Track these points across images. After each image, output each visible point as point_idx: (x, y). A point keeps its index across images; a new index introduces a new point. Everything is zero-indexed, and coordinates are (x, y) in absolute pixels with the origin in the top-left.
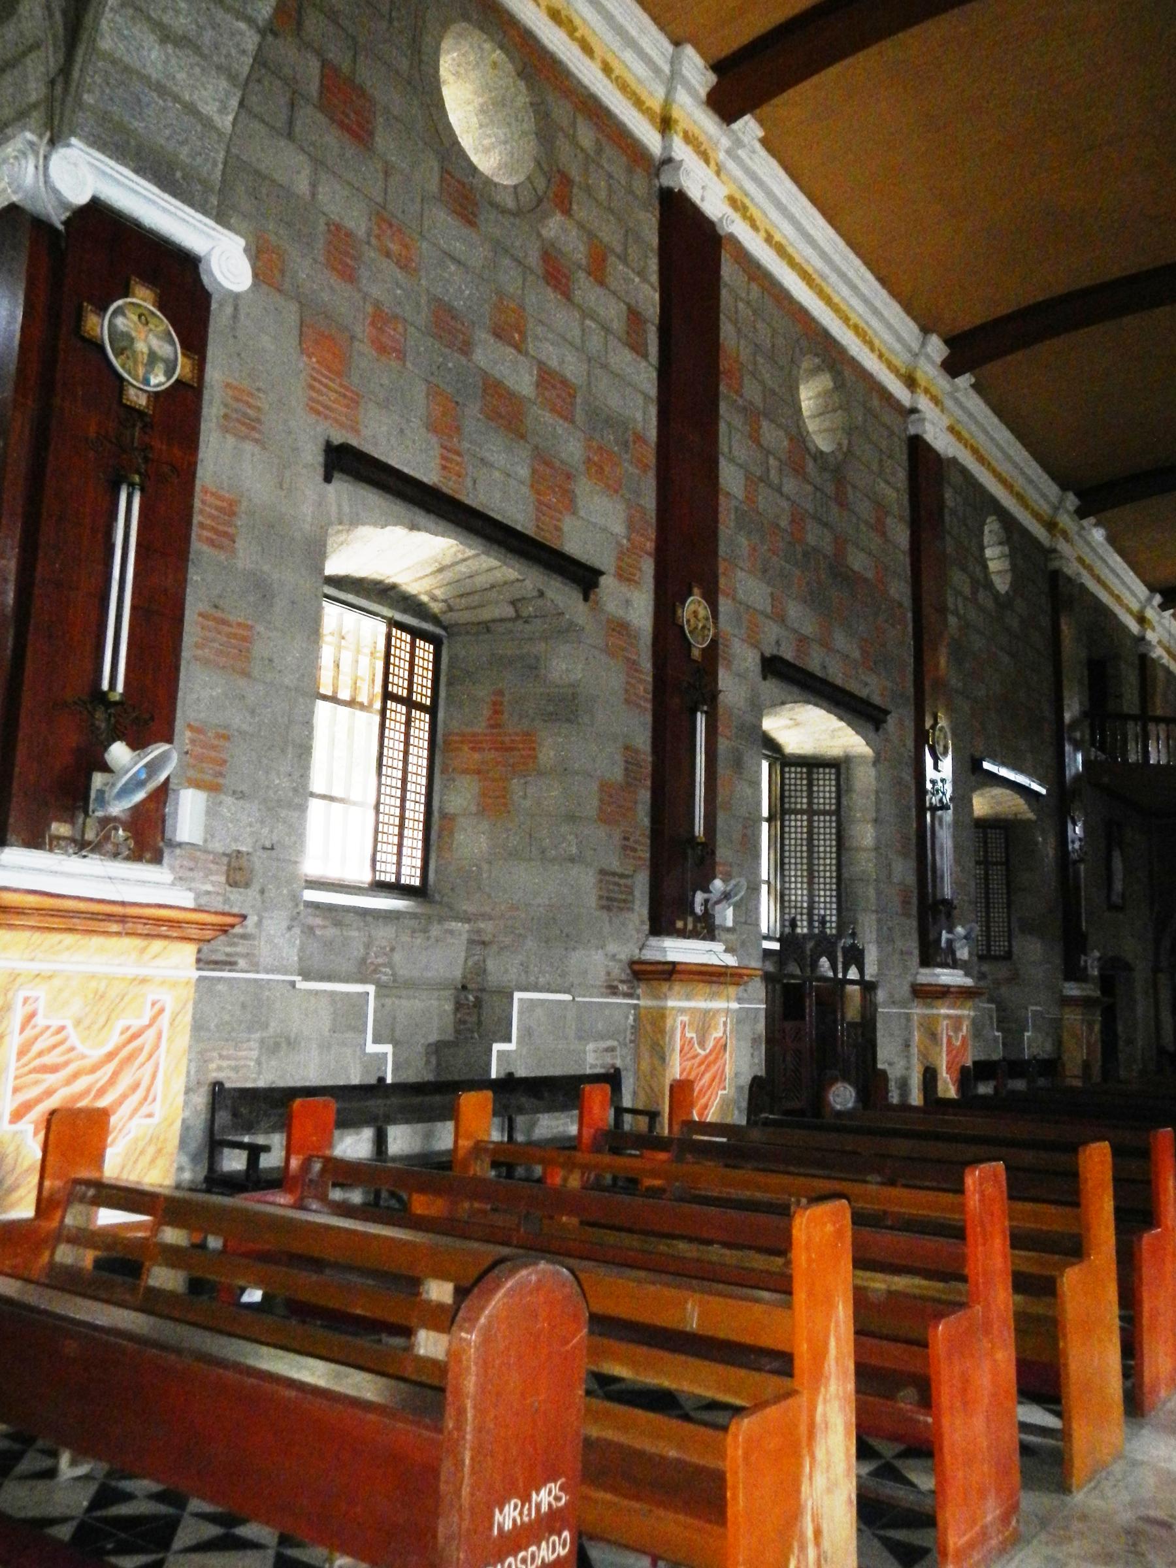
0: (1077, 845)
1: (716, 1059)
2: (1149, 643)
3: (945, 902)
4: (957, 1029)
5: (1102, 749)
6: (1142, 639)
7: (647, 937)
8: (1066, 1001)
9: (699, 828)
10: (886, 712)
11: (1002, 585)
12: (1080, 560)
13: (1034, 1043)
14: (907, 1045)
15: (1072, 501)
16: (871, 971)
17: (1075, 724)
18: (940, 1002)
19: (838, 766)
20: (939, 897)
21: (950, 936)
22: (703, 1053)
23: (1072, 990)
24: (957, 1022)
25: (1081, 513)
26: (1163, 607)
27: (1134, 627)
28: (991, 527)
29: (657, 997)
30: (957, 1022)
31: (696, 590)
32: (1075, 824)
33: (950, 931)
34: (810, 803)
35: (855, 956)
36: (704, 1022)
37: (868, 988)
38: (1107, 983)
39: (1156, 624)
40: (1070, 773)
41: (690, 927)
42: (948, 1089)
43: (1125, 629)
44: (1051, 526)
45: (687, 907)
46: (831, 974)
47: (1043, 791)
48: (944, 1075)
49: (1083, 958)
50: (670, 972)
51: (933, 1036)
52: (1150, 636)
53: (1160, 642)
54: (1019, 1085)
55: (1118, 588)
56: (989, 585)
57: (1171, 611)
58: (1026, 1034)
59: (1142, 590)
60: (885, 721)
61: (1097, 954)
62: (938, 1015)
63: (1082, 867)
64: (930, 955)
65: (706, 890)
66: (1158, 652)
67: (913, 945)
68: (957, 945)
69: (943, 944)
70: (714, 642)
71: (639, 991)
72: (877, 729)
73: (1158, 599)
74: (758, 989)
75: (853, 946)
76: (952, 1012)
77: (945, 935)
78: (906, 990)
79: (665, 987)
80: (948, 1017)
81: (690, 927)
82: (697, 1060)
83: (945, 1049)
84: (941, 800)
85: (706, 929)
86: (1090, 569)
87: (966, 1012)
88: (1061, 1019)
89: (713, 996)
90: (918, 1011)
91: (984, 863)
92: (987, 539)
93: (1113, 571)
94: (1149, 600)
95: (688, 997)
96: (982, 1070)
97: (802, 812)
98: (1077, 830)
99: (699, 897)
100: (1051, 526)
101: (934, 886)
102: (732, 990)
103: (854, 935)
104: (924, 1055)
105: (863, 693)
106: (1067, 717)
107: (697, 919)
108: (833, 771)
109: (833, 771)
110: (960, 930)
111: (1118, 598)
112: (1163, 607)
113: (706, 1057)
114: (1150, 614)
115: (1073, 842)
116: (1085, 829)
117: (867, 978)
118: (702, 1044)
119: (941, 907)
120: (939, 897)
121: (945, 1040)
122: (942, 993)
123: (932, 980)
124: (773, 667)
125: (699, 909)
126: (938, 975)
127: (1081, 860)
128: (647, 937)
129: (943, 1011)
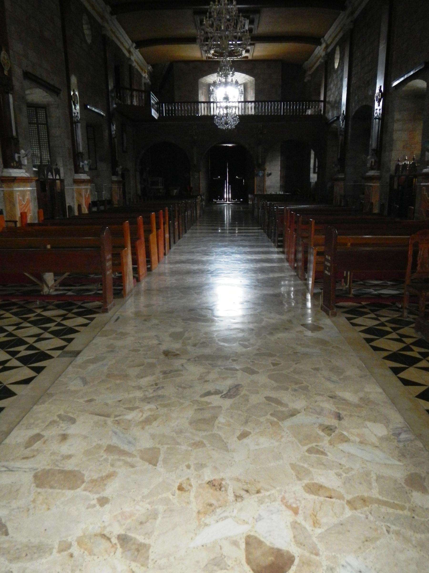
0: (114, 132)
1: (28, 205)
2: (132, 61)
3: (80, 153)
4: (87, 192)
5: (120, 100)
6: (130, 59)
7: (3, 169)
8: (113, 182)
9: (14, 133)
10: (60, 90)
11: (89, 41)
12: (112, 30)
13: (105, 195)
14: (73, 198)
15: (109, 9)
16: (62, 175)
17: (112, 91)
18: (81, 185)
19: (44, 107)
20: (79, 151)
21: (83, 164)
22: (24, 203)
23: (115, 178)
24: (86, 189)
25: (112, 13)
26: (136, 48)
27: (127, 54)
28: (85, 17)
29: (9, 187)
30: (86, 189)
31: (3, 49)
32: (113, 125)
33: (83, 162)
34: (37, 120)
35: (58, 172)
36: (23, 193)
37: (62, 181)
38: (123, 176)
39: (133, 53)
40: (111, 108)
41: (15, 165)
42: (85, 210)
43: (124, 55)
44: (103, 18)
45: (13, 159)
46: (52, 178)
47: (105, 115)
48: (84, 206)
49: (117, 168)
50: (14, 180)
51: (80, 195)
52: (133, 58)
53: (135, 60)
54: (102, 208)
55: (122, 39)
56: (86, 41)
57: (138, 49)
58: (103, 193)
59: (130, 42)
60: (60, 93)
61: (121, 167)
62: (81, 189)
63: (116, 139)
64: (77, 170)
65: (18, 153)
66: (134, 64)
67: (72, 167)
68: (85, 167)
69: (81, 166)
70: (10, 68)
71: (3, 186)
72: (57, 96)
73: (134, 45)
74: (34, 184)
75: (57, 168)
76: (85, 187)
77: (81, 164)
78: (71, 181)
79: (12, 184)
80: (84, 189)
81: (15, 165)
82: (23, 206)
83: (84, 198)
84: (77, 120)
85: (19, 166)
86: (114, 33)
87: (89, 187)
88: (112, 188)
89: (24, 186)
90: (75, 187)
91: (88, 139)
92: (84, 22)
93: (121, 34)
94: (132, 45)
95: (19, 187)
96: (94, 204)
97: (34, 124)
98: (114, 128)
99: (17, 155)
100: (103, 18)
101: (77, 148)
102: (29, 184)
103: (57, 165)
104: (78, 201)
105: (52, 83)
106: (110, 88)
107: (17, 162)
108: (44, 109)
109: (44, 109)
110: (86, 162)
111: (122, 43)
112: (136, 48)
113: (25, 204)
114: (132, 50)
115: (113, 131)
116: (116, 127)
117: (61, 178)
118: (24, 201)
119: (80, 155)
120: (79, 151)
121: (84, 196)
122: (83, 182)
123: (79, 178)
124: (27, 75)
125: (17, 159)
126: (81, 176)
127: (115, 137)
128: (3, 169)
129: (83, 187)
